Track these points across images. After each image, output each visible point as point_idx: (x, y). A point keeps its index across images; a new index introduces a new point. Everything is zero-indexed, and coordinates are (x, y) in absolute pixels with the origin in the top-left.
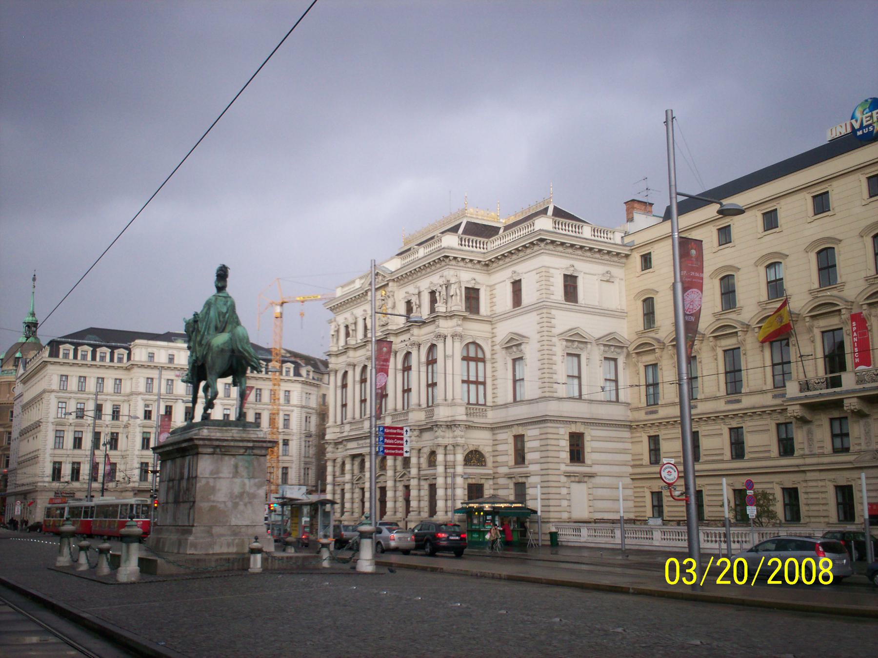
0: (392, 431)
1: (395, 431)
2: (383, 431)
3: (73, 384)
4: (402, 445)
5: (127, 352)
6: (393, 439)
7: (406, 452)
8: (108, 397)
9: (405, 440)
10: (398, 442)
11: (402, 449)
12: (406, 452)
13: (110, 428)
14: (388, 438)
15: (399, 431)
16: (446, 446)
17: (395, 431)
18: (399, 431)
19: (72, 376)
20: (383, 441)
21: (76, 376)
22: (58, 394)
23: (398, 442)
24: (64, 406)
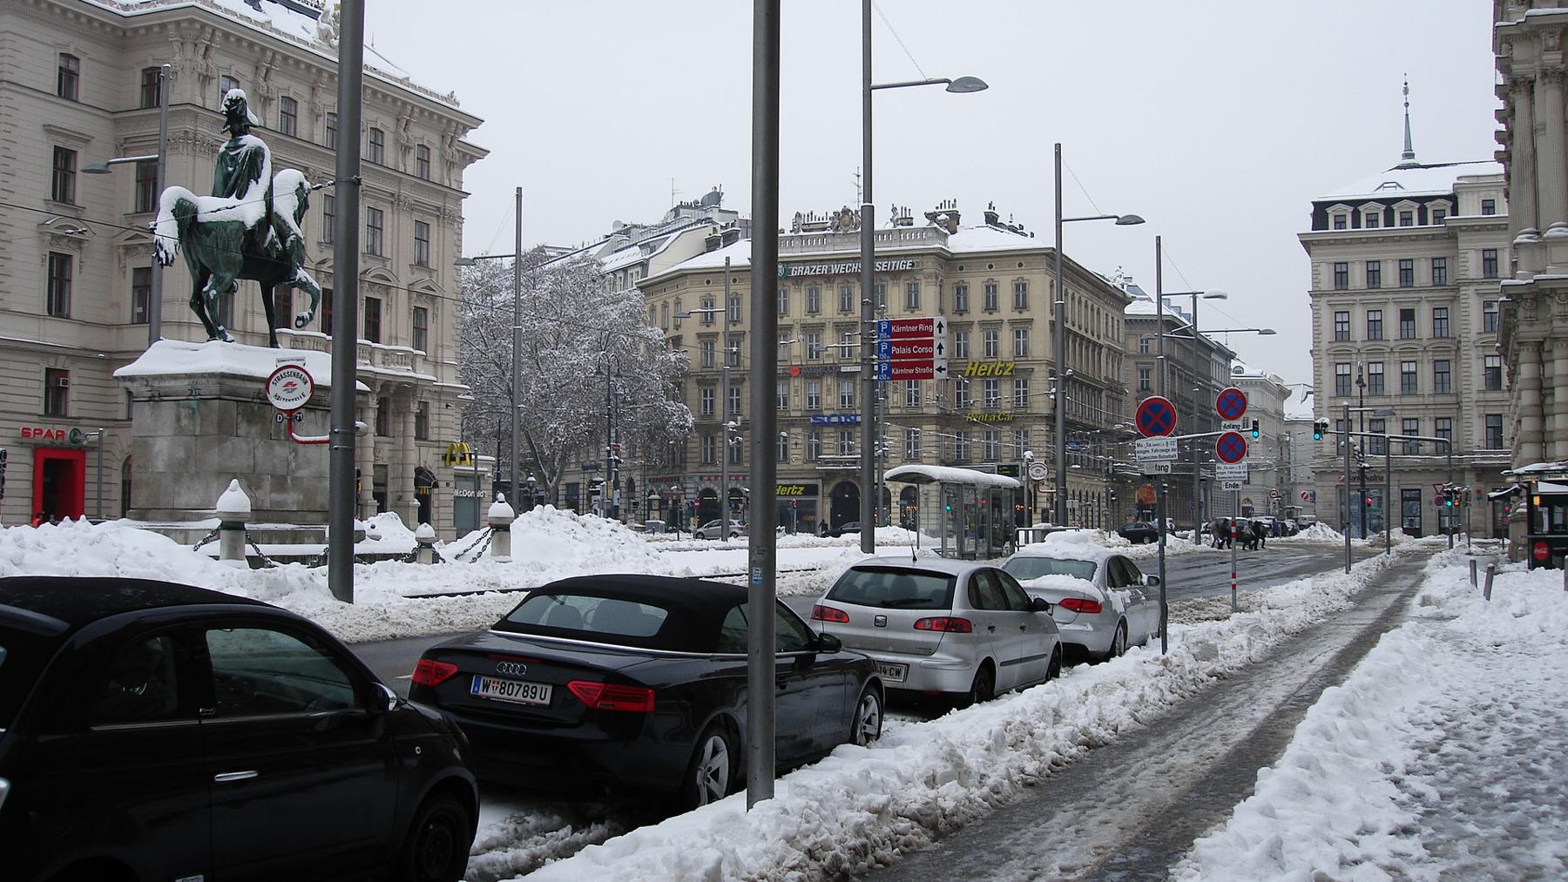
0: (907, 328)
1: (914, 329)
2: (888, 331)
3: (1357, 277)
4: (931, 355)
5: (1450, 204)
6: (910, 344)
7: (940, 369)
8: (1390, 296)
9: (936, 345)
10: (921, 350)
11: (931, 364)
12: (940, 369)
13: (1430, 353)
14: (897, 344)
15: (921, 327)
16: (1541, 343)
17: (914, 329)
18: (921, 327)
19: (1354, 262)
20: (888, 352)
21: (1361, 262)
22: (1331, 298)
23: (921, 350)
24: (1378, 318)
